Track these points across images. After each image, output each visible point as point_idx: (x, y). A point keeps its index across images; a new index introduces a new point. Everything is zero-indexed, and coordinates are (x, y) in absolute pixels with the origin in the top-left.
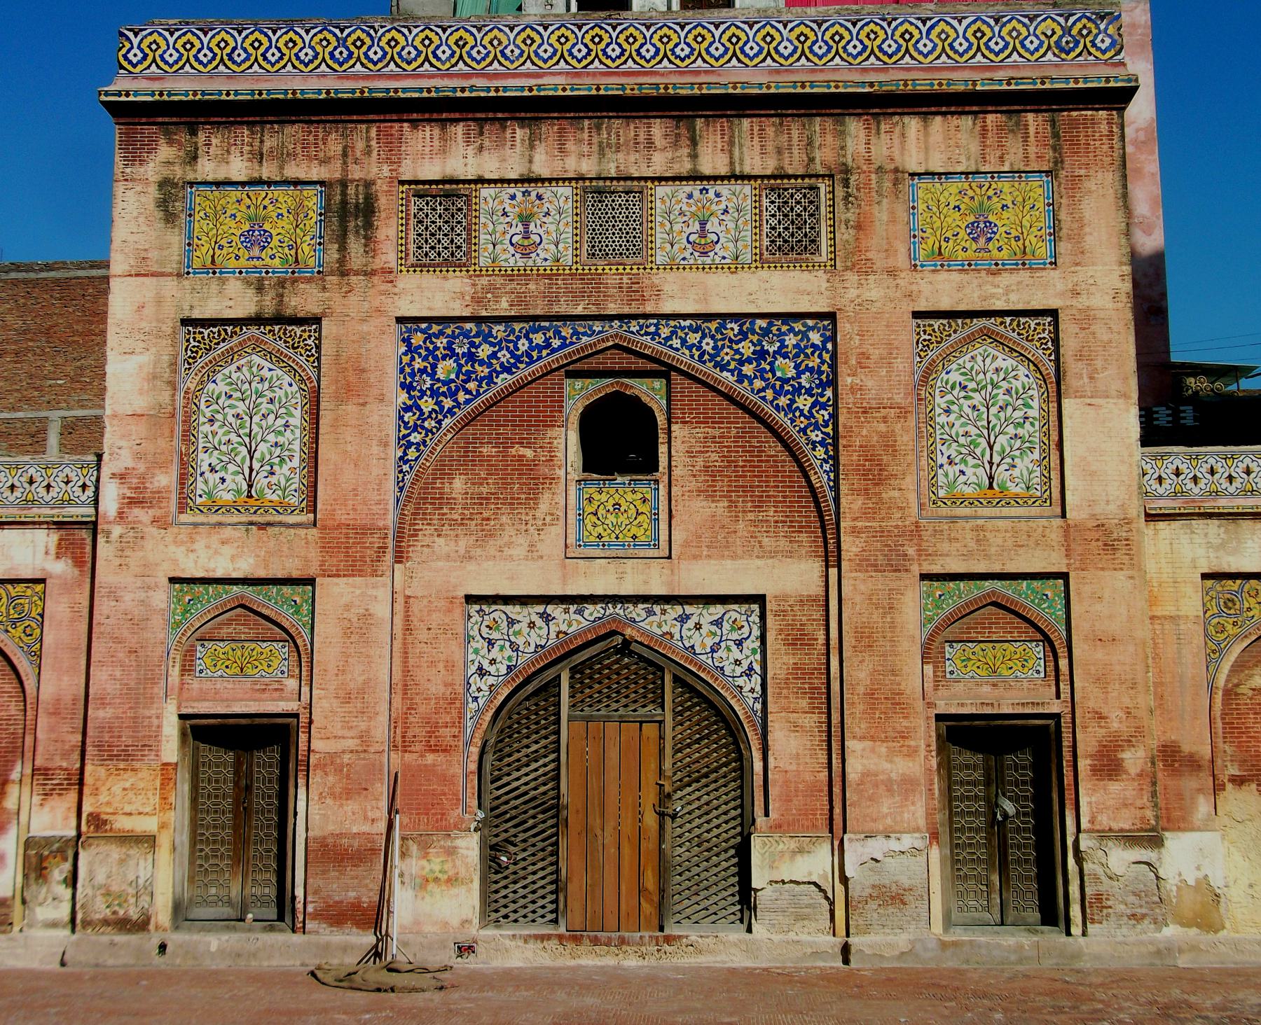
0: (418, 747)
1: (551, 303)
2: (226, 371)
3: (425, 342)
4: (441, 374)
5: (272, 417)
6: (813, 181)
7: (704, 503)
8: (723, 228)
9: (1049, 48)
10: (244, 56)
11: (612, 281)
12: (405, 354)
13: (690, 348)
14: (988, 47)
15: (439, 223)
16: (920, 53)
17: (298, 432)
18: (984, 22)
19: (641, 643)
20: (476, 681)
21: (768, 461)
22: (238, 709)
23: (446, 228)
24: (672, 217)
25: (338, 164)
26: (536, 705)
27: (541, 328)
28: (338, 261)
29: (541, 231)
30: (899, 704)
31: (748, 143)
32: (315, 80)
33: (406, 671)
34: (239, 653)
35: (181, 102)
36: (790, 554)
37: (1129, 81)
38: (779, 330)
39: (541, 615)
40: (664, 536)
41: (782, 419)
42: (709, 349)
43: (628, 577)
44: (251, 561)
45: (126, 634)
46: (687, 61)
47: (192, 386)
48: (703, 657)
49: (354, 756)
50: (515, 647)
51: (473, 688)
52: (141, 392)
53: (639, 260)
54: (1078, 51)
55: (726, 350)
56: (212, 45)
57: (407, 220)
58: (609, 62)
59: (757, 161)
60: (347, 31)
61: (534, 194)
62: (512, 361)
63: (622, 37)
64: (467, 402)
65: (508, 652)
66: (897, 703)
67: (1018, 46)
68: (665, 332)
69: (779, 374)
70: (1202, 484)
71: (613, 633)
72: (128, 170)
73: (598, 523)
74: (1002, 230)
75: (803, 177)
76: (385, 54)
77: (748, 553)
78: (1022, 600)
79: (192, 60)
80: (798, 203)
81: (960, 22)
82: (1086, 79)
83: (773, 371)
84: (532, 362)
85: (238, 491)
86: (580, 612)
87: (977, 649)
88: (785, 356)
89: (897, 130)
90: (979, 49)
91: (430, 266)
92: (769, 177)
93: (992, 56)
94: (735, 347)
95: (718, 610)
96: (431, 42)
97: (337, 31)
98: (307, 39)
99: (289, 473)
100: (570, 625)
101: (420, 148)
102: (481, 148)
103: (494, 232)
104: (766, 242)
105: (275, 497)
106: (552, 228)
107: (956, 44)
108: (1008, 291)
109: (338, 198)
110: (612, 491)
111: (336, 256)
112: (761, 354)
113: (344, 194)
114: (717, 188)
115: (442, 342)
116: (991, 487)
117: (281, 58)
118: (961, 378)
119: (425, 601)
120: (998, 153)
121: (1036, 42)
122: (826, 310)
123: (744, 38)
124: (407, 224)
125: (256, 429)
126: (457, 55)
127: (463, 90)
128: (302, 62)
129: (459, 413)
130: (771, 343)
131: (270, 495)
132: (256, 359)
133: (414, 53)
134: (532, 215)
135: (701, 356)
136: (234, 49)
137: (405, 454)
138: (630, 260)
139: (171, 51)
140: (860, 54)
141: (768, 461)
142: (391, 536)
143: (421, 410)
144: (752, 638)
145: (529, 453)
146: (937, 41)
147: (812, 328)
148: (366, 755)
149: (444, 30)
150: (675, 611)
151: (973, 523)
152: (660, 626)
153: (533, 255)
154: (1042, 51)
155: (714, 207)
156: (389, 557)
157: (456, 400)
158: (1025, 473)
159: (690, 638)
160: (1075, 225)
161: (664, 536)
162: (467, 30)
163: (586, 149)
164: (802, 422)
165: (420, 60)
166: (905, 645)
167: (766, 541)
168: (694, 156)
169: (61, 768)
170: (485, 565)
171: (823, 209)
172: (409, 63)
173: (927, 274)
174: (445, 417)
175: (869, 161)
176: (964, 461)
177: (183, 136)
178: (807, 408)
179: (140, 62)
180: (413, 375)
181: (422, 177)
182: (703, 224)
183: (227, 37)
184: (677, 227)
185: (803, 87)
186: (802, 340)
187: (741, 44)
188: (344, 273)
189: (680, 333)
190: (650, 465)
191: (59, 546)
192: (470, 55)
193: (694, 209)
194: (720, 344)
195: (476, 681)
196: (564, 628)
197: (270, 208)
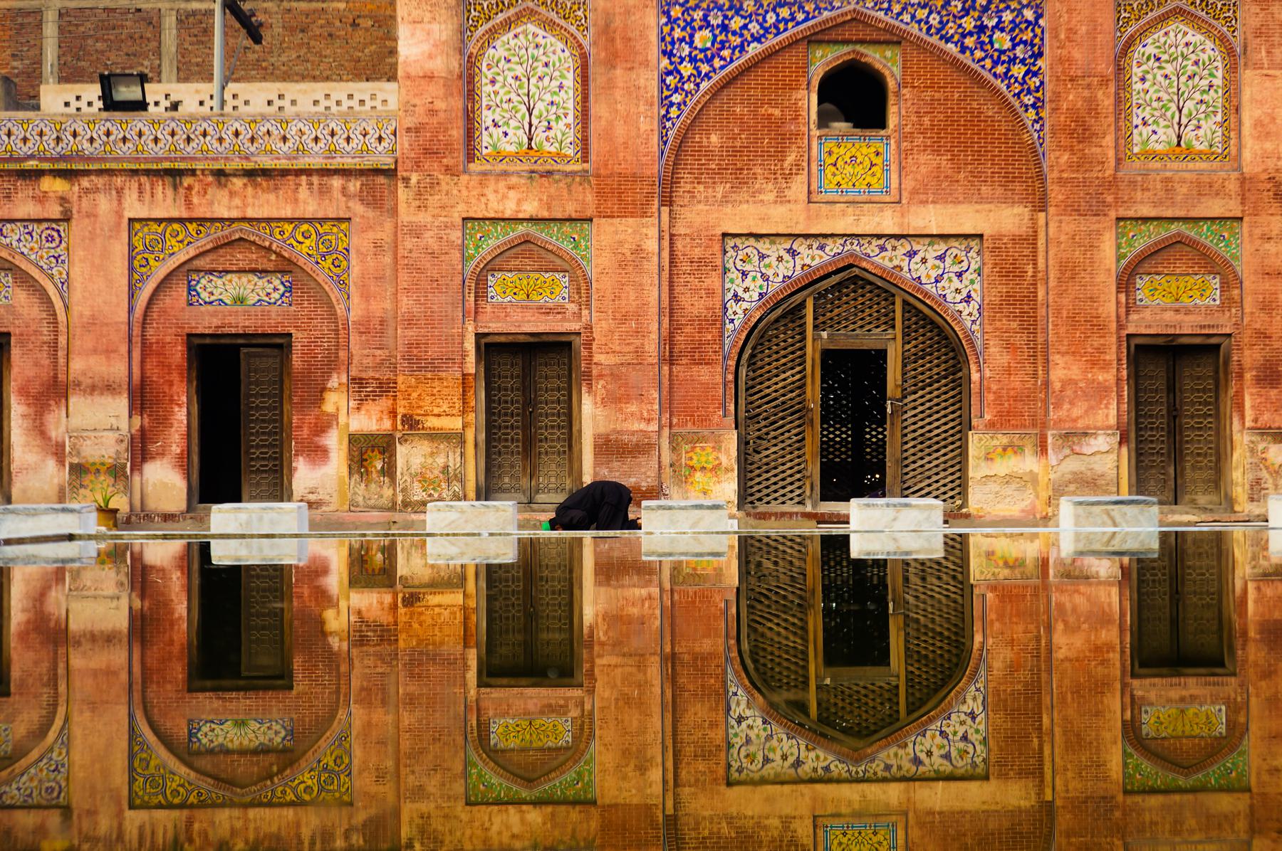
2: (505, 38)
4: (698, 43)
12: (666, 24)
13: (919, 22)
17: (571, 93)
20: (731, 306)
36: (1004, 200)
39: (788, 251)
44: (536, 204)
47: (475, 52)
48: (928, 287)
50: (765, 278)
51: (730, 312)
62: (762, 32)
64: (722, 67)
65: (760, 282)
66: (1097, 325)
69: (996, 46)
71: (851, 266)
77: (967, 199)
78: (1202, 240)
83: (991, 43)
85: (520, 144)
86: (822, 248)
88: (1002, 30)
95: (941, 247)
100: (813, 258)
105: (552, 149)
110: (850, 145)
112: (981, 29)
115: (698, 15)
116: (1179, 144)
118: (1156, 51)
129: (716, 78)
130: (990, 18)
131: (547, 147)
132: (531, 28)
137: (668, 112)
144: (971, 270)
145: (777, 112)
150: (904, 247)
152: (891, 260)
157: (712, 66)
158: (1209, 134)
161: (894, 184)
166: (1101, 278)
189: (910, 9)
194: (945, 19)
196: (808, 261)
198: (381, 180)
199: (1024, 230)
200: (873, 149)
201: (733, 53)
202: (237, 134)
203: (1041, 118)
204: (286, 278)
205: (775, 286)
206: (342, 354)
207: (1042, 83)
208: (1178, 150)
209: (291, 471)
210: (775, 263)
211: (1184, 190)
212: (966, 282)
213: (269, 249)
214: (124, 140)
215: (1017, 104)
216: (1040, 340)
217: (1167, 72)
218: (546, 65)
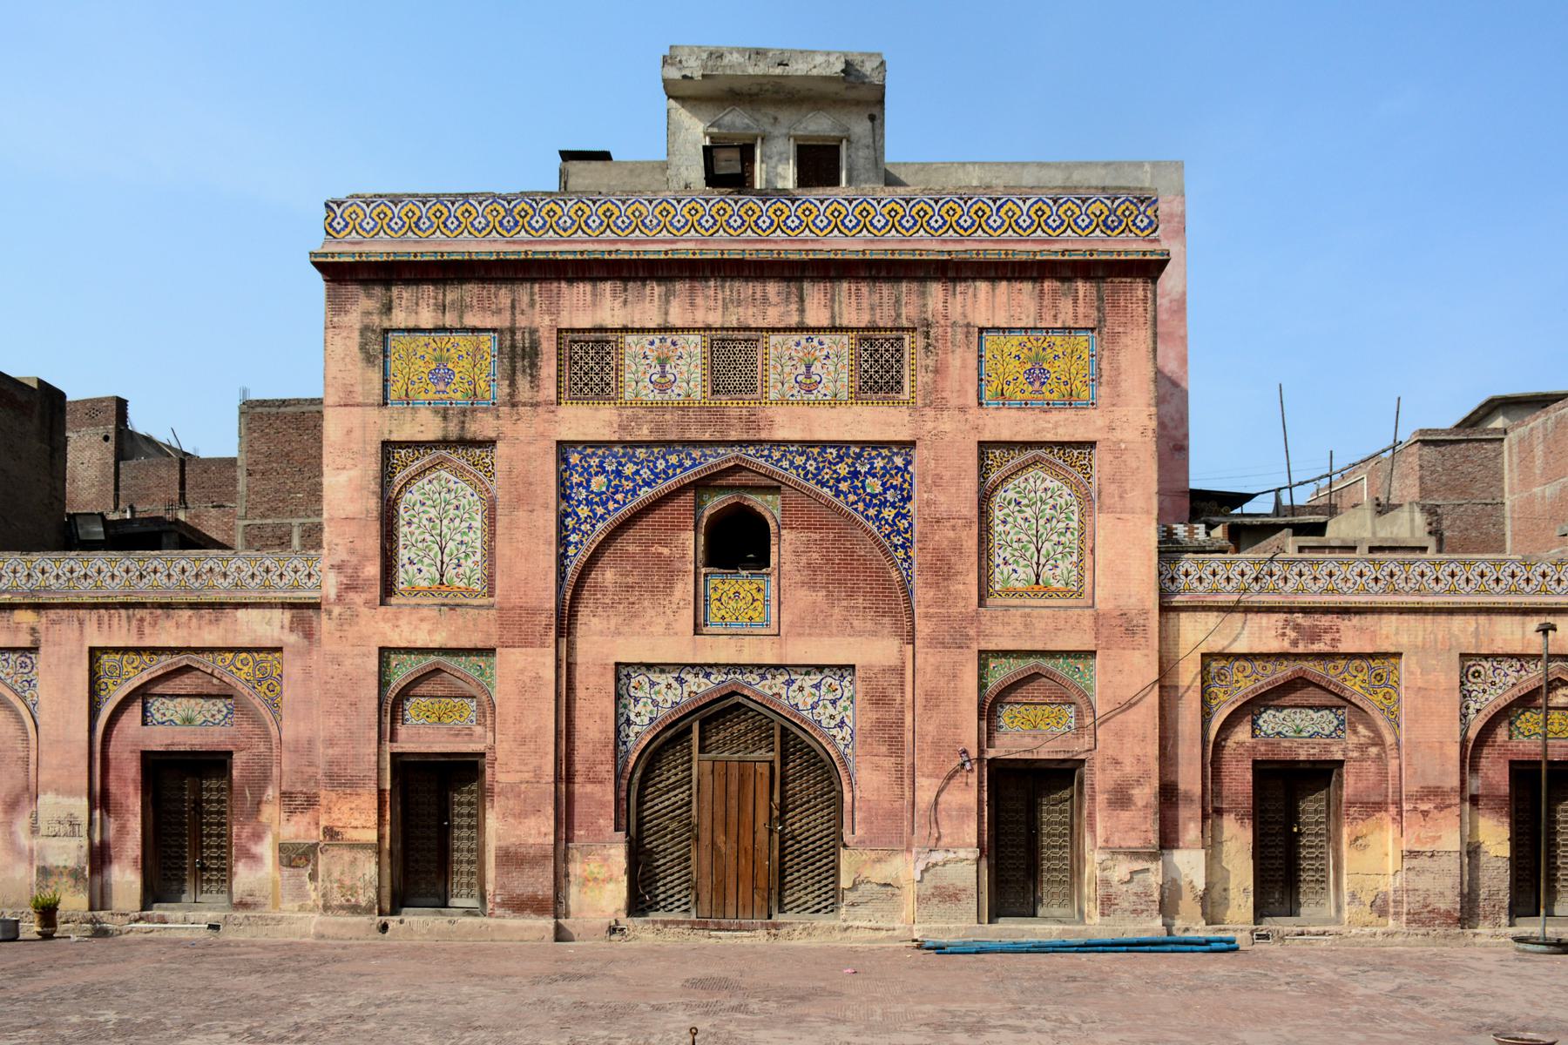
2: (420, 484)
4: (594, 487)
5: (458, 520)
6: (900, 333)
9: (1098, 225)
10: (428, 223)
11: (734, 412)
13: (797, 468)
14: (1047, 224)
15: (591, 364)
16: (991, 227)
17: (479, 533)
18: (1044, 203)
22: (437, 749)
23: (597, 369)
25: (508, 314)
28: (509, 394)
29: (674, 371)
31: (845, 300)
32: (488, 244)
34: (437, 706)
35: (376, 262)
36: (874, 633)
37: (1162, 254)
39: (676, 679)
42: (812, 469)
43: (746, 650)
45: (346, 690)
46: (797, 231)
48: (805, 713)
49: (530, 786)
51: (623, 734)
52: (352, 500)
53: (755, 396)
54: (1121, 229)
55: (826, 470)
56: (402, 215)
58: (731, 231)
59: (854, 316)
60: (513, 203)
63: (743, 210)
64: (616, 510)
65: (650, 707)
67: (1072, 223)
69: (868, 490)
70: (1205, 584)
71: (733, 693)
72: (336, 319)
74: (1053, 376)
75: (891, 330)
76: (545, 222)
78: (1059, 672)
79: (385, 227)
80: (887, 351)
81: (1024, 202)
82: (1126, 252)
83: (864, 488)
85: (433, 580)
86: (707, 675)
87: (1022, 709)
88: (874, 476)
89: (971, 291)
90: (1039, 225)
92: (863, 329)
93: (1050, 231)
96: (584, 212)
97: (505, 203)
98: (480, 210)
99: (472, 566)
100: (699, 686)
102: (625, 302)
103: (637, 371)
105: (462, 585)
106: (685, 369)
107: (1020, 221)
108: (1056, 426)
109: (508, 343)
110: (733, 582)
111: (508, 391)
112: (855, 474)
113: (513, 340)
115: (594, 461)
116: (1037, 583)
117: (459, 226)
118: (1017, 496)
120: (1053, 312)
121: (1087, 221)
122: (908, 439)
123: (845, 213)
125: (445, 530)
126: (605, 224)
127: (610, 253)
128: (477, 229)
129: (610, 519)
130: (863, 465)
132: (444, 474)
133: (569, 222)
134: (668, 358)
135: (806, 474)
136: (420, 218)
137: (566, 551)
138: (748, 396)
139: (369, 220)
140: (940, 227)
145: (666, 551)
146: (1005, 217)
147: (897, 454)
149: (594, 203)
151: (1021, 611)
152: (770, 688)
154: (1091, 228)
155: (817, 353)
157: (606, 509)
158: (1065, 572)
160: (1113, 373)
161: (774, 618)
162: (613, 203)
163: (712, 303)
164: (887, 529)
165: (575, 228)
167: (856, 623)
168: (802, 311)
169: (301, 792)
171: (907, 356)
172: (565, 230)
173: (991, 411)
175: (946, 317)
176: (1016, 562)
177: (378, 291)
179: (343, 229)
181: (577, 326)
182: (808, 367)
183: (414, 208)
184: (787, 370)
185: (893, 254)
187: (842, 217)
188: (514, 405)
189: (789, 456)
190: (763, 560)
191: (292, 622)
192: (616, 225)
193: (801, 354)
194: (821, 465)
196: (694, 688)
197: (452, 350)
198: (311, 612)
199: (894, 661)
202: (183, 571)
203: (910, 557)
204: (229, 701)
205: (664, 712)
206: (275, 771)
208: (1036, 587)
209: (231, 875)
211: (1042, 625)
213: (212, 675)
214: (86, 576)
215: (887, 544)
217: (1026, 515)
218: (457, 508)
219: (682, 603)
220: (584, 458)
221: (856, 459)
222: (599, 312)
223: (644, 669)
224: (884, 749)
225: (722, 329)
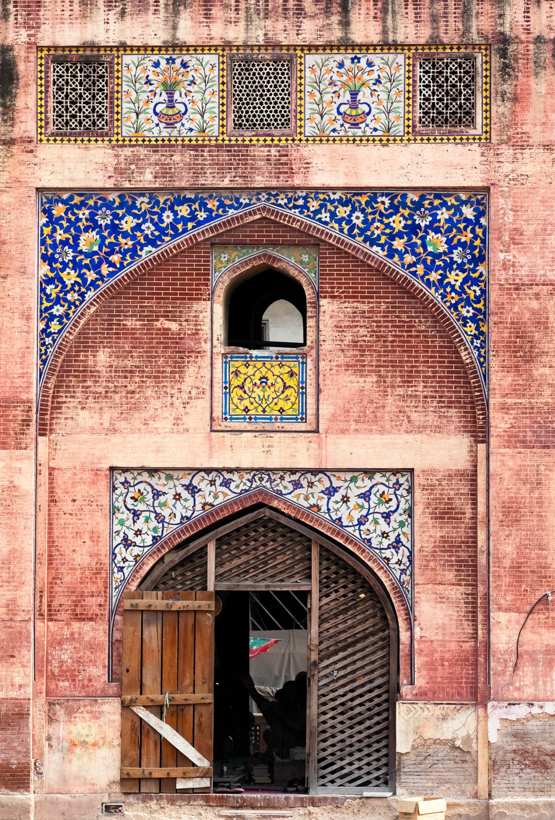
0: (63, 616)
1: (196, 175)
3: (66, 213)
4: (83, 246)
7: (353, 378)
8: (375, 99)
12: (46, 225)
13: (339, 222)
15: (80, 90)
19: (288, 516)
20: (121, 552)
21: (418, 336)
23: (87, 96)
24: (322, 87)
26: (183, 575)
27: (186, 200)
29: (185, 100)
30: (545, 577)
33: (51, 542)
36: (438, 429)
38: (431, 204)
40: (311, 411)
41: (433, 293)
42: (358, 222)
43: (275, 451)
48: (350, 530)
50: (160, 518)
51: (119, 558)
53: (287, 131)
57: (47, 87)
59: (411, 30)
61: (178, 62)
62: (157, 233)
64: (111, 275)
65: (154, 523)
68: (314, 205)
69: (430, 249)
71: (260, 505)
73: (245, 396)
80: (454, 73)
83: (424, 246)
84: (177, 234)
86: (226, 483)
88: (437, 231)
91: (71, 135)
94: (386, 221)
95: (365, 484)
100: (216, 497)
101: (59, 12)
102: (123, 14)
103: (138, 100)
104: (419, 113)
106: (197, 97)
112: (413, 229)
114: (370, 57)
115: (83, 214)
119: (69, 474)
122: (480, 184)
124: (47, 92)
129: (103, 286)
130: (423, 217)
135: (351, 230)
137: (48, 326)
141: (418, 336)
142: (34, 409)
143: (63, 282)
144: (400, 511)
145: (174, 326)
147: (465, 203)
148: (13, 624)
152: (307, 498)
153: (178, 125)
155: (366, 77)
156: (33, 429)
157: (99, 273)
159: (337, 510)
163: (233, 15)
164: (454, 298)
167: (414, 416)
168: (345, 24)
170: (130, 437)
174: (88, 289)
175: (528, 31)
178: (458, 284)
180: (54, 246)
182: (354, 94)
184: (327, 98)
186: (454, 214)
189: (329, 207)
193: (345, 78)
194: (370, 217)
195: (121, 552)
196: (210, 500)
200: (287, 369)
201: (124, 259)
203: (482, 333)
207: (483, 292)
210: (171, 502)
212: (394, 524)
216: (481, 589)
219: (194, 392)
220: (70, 209)
221: (415, 210)
222: (89, 25)
223: (145, 476)
224: (450, 575)
225: (246, 46)
